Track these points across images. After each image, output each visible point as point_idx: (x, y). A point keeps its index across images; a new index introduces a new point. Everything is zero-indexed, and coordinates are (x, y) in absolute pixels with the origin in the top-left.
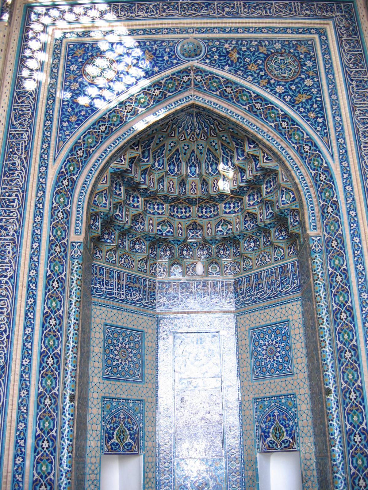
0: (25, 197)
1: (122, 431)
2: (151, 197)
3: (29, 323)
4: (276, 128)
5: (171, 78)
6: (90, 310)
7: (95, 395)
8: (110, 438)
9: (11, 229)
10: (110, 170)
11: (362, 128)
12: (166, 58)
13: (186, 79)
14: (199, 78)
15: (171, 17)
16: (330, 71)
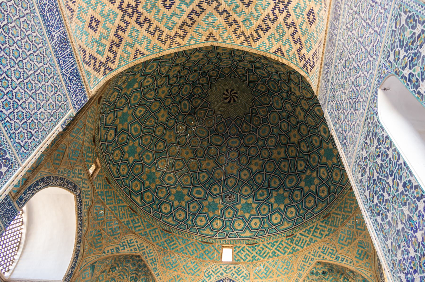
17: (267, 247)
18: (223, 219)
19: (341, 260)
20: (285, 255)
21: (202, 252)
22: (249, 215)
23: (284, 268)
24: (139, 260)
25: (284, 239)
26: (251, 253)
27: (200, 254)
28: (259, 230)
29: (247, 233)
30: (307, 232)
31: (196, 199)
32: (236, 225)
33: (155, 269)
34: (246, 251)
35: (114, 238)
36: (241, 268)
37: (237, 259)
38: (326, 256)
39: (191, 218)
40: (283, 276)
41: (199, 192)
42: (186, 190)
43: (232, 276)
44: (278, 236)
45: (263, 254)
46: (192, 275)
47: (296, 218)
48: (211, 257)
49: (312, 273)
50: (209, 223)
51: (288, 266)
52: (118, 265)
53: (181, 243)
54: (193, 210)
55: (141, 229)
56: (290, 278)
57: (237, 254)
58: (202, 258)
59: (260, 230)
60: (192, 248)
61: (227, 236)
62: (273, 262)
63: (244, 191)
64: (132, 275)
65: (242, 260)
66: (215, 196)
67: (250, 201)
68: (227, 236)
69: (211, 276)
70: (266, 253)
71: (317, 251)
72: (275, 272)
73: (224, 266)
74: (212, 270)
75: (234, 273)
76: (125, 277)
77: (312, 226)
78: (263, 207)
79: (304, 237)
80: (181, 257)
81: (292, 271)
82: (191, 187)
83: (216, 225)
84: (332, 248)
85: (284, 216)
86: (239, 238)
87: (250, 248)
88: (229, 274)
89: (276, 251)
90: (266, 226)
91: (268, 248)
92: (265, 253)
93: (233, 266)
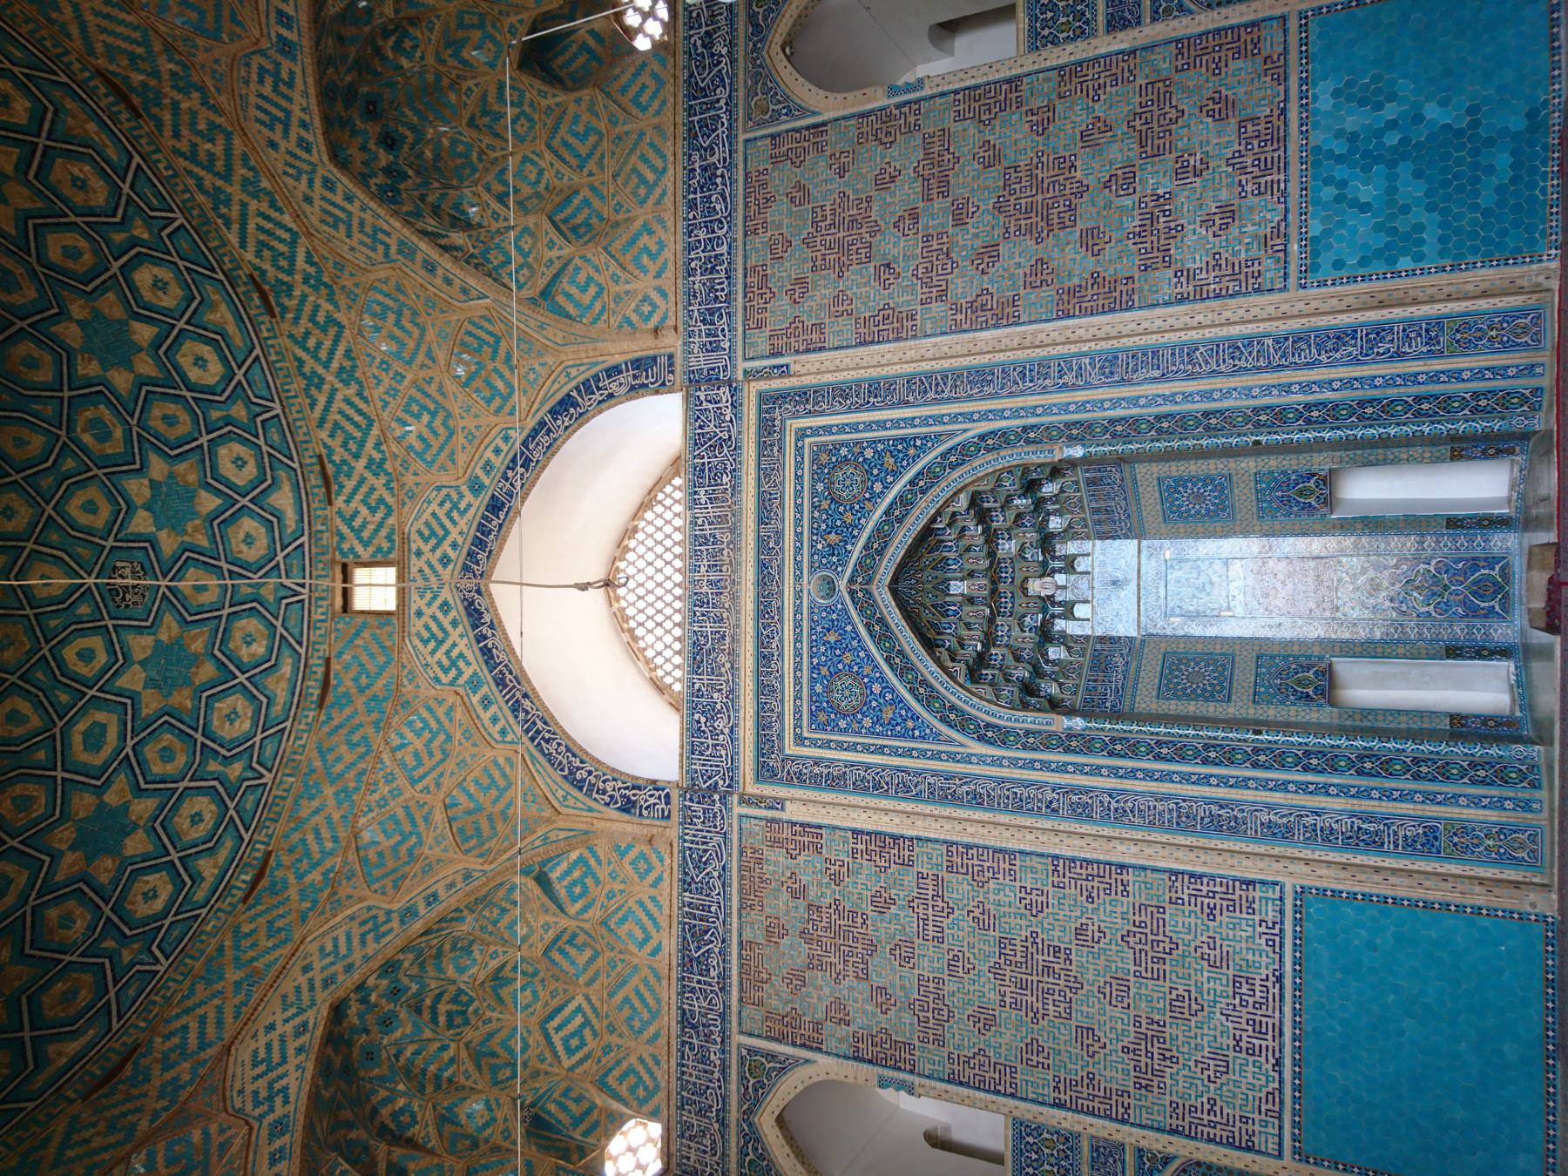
0: (1011, 780)
1: (1299, 682)
2: (990, 640)
3: (1166, 777)
4: (923, 492)
5: (861, 611)
6: (1141, 714)
7: (1251, 711)
8: (1308, 695)
9: (1050, 795)
10: (968, 685)
11: (931, 395)
12: (834, 616)
13: (860, 595)
14: (860, 579)
15: (780, 610)
16: (854, 428)
17: (327, 409)
18: (225, 612)
19: (289, 28)
20: (345, 322)
21: (360, 702)
22: (204, 494)
23: (397, 332)
24: (364, 1000)
25: (285, 326)
26: (362, 481)
27: (370, 711)
28: (265, 448)
29: (283, 499)
30: (224, 210)
31: (129, 749)
32: (251, 554)
33: (409, 913)
34: (353, 505)
35: (221, 1158)
36: (420, 525)
37: (386, 545)
38: (297, 113)
39: (213, 766)
40: (431, 335)
41: (94, 738)
42: (75, 800)
43: (449, 561)
44: (273, 358)
45: (357, 425)
46: (449, 739)
47: (181, 263)
48: (382, 660)
49: (389, 196)
50: (242, 678)
51: (386, 308)
52: (386, 1101)
53: (315, 804)
54: (181, 760)
55: (219, 1010)
56: (428, 299)
57: (366, 545)
58: (385, 699)
59: (261, 442)
60: (343, 748)
61: (297, 594)
62: (379, 382)
63: (91, 517)
64: (442, 1019)
65: (391, 521)
66: (120, 659)
67: (137, 488)
68: (297, 594)
69: (454, 654)
70: (350, 412)
71: (288, 158)
72: (422, 374)
73: (417, 602)
74: (433, 653)
75: (439, 553)
76: (447, 1055)
77: (191, 182)
78: (162, 428)
79: (251, 227)
80: (376, 796)
81: (399, 288)
82: (60, 774)
83: (254, 646)
84: (255, 77)
85: (181, 324)
86: (305, 539)
87: (342, 486)
88: (446, 574)
89: (335, 365)
90: (243, 413)
91: (330, 401)
92: (349, 419)
93: (414, 559)
